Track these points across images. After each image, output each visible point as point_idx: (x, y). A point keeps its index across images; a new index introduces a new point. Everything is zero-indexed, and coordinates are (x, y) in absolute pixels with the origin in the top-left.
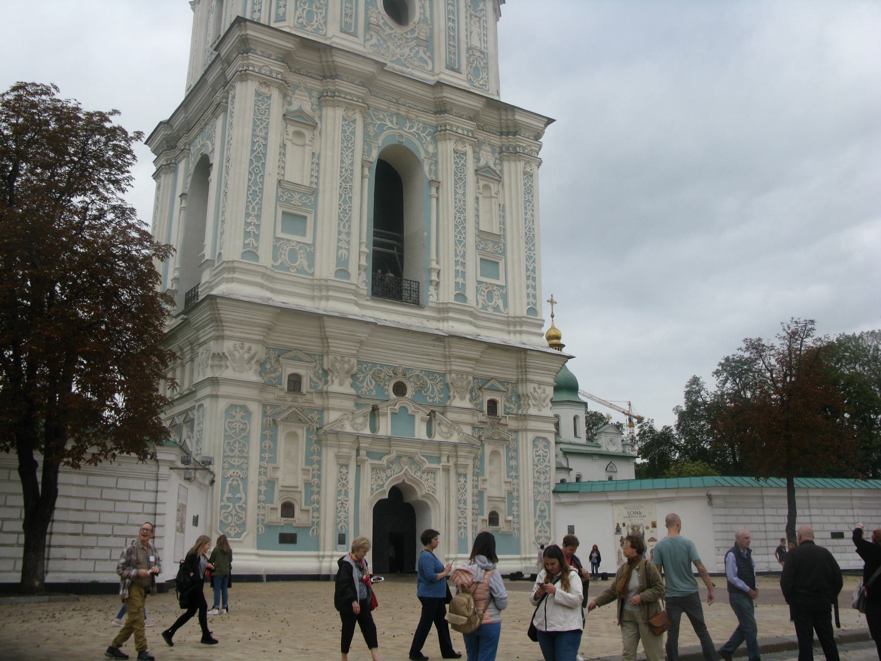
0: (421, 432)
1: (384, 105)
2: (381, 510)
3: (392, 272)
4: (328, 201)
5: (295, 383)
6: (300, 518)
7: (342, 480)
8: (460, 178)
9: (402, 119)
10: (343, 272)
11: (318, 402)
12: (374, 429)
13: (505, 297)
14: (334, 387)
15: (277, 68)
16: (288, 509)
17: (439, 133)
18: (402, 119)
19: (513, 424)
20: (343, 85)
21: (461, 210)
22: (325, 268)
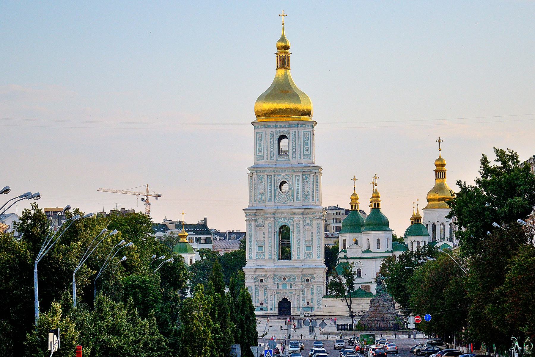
0: (289, 287)
1: (279, 216)
2: (280, 303)
3: (285, 254)
4: (267, 243)
5: (262, 281)
6: (264, 305)
7: (271, 298)
8: (298, 230)
9: (284, 219)
10: (270, 258)
11: (267, 284)
12: (278, 288)
13: (312, 255)
14: (269, 281)
15: (253, 217)
16: (262, 304)
17: (293, 219)
18: (284, 219)
19: (313, 283)
20: (267, 216)
21: (298, 237)
22: (267, 257)
